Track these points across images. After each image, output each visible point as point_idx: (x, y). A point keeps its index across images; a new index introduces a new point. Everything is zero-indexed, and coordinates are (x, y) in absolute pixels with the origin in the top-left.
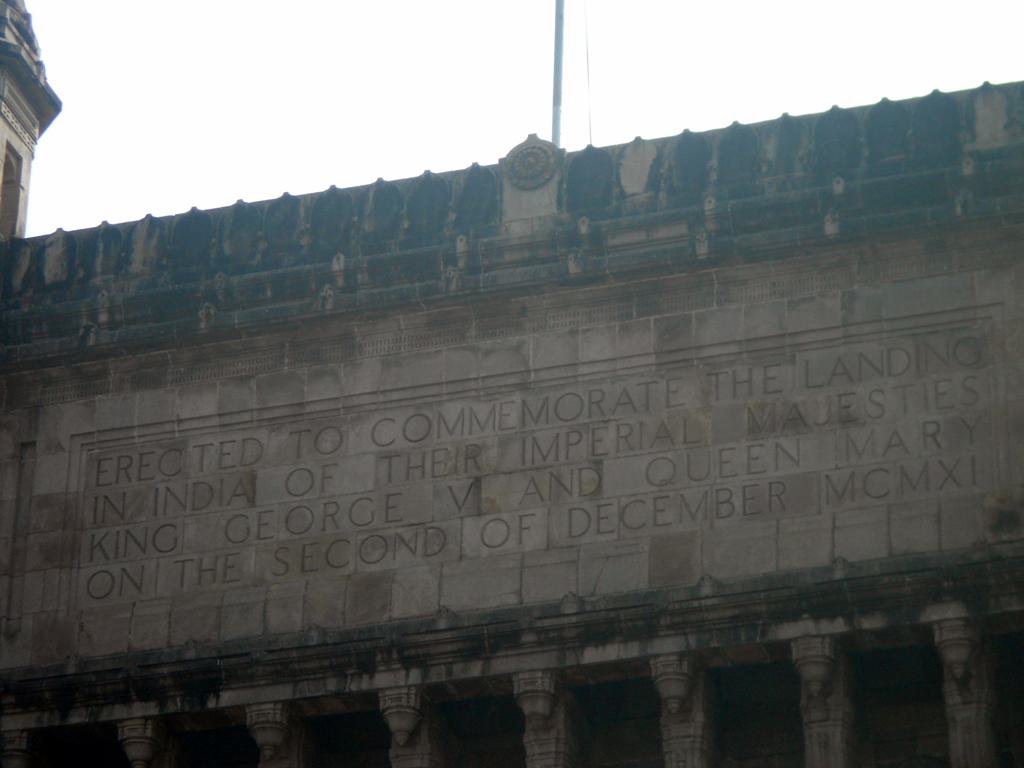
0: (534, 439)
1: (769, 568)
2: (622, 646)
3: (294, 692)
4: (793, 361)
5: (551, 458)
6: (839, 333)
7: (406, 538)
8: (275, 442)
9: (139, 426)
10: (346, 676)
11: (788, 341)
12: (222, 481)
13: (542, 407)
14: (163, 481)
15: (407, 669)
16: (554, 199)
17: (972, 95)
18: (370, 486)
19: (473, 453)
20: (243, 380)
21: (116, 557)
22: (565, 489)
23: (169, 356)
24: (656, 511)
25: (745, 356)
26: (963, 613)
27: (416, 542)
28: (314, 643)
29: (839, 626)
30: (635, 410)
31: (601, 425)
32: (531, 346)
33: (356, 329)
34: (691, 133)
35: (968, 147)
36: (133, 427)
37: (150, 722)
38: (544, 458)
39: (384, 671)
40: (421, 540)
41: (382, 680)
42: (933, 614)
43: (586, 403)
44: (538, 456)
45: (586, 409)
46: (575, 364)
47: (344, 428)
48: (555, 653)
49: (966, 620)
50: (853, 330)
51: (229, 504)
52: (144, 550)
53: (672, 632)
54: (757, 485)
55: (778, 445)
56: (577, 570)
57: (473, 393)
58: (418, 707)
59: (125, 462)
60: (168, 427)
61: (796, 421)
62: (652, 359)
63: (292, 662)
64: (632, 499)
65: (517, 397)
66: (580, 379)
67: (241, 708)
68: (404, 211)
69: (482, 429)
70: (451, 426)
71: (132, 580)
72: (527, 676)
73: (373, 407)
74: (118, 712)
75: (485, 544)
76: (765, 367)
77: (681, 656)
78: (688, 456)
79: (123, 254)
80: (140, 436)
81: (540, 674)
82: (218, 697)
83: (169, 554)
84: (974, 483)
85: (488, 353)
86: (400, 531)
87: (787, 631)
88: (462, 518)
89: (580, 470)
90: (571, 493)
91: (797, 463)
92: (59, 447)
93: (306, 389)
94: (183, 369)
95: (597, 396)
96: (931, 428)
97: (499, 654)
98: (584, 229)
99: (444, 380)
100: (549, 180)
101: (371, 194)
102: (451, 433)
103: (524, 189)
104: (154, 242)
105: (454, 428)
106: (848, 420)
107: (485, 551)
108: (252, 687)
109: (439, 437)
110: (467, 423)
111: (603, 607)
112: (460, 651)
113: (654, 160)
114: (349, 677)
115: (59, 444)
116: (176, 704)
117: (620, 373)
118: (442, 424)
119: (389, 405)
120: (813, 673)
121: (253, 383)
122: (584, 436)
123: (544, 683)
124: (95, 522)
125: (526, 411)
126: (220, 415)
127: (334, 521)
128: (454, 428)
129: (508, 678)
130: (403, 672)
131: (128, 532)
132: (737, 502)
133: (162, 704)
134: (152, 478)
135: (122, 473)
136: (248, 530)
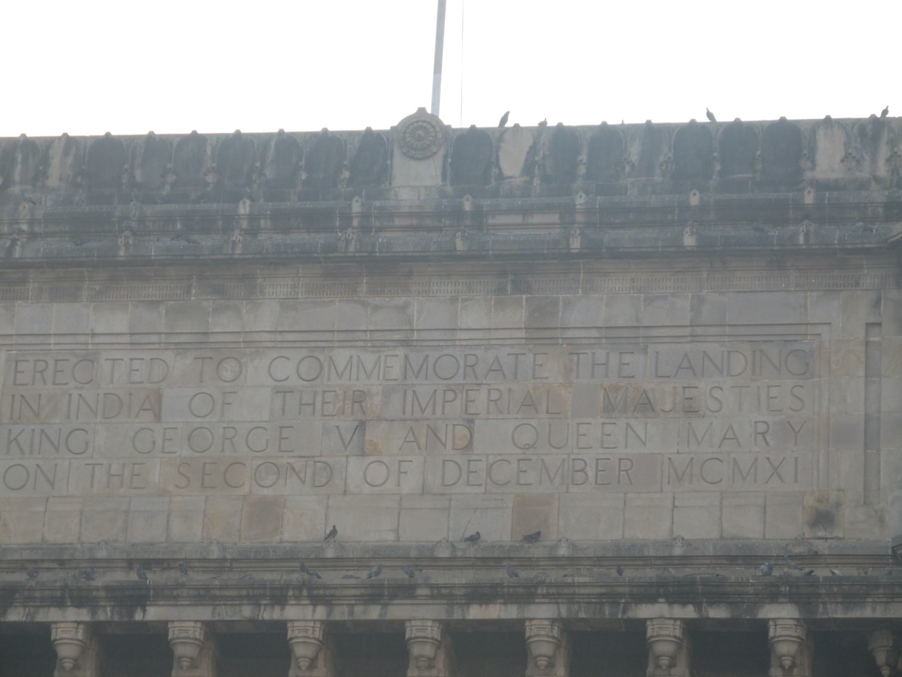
0: (414, 392)
1: (616, 535)
2: (503, 607)
3: (213, 613)
4: (645, 351)
5: (429, 410)
6: (687, 331)
9: (55, 335)
10: (259, 605)
11: (642, 332)
12: (131, 394)
14: (76, 388)
15: (315, 605)
16: (439, 172)
17: (816, 125)
19: (360, 398)
20: (153, 304)
21: (31, 452)
22: (441, 441)
25: (604, 341)
26: (796, 615)
27: (306, 473)
28: (215, 556)
29: (689, 612)
30: (505, 377)
31: (475, 387)
32: (416, 307)
33: (259, 271)
35: (808, 175)
36: (50, 335)
37: (81, 626)
38: (423, 411)
41: (291, 612)
42: (769, 612)
43: (462, 364)
44: (417, 408)
45: (461, 371)
48: (445, 606)
49: (797, 620)
50: (699, 331)
51: (136, 416)
52: (57, 450)
53: (547, 601)
54: (609, 459)
55: (628, 424)
56: (449, 516)
57: (362, 344)
58: (321, 638)
59: (41, 366)
60: (82, 339)
62: (522, 334)
63: (213, 589)
64: (499, 458)
65: (401, 352)
66: (457, 343)
67: (165, 623)
68: (303, 163)
69: (369, 377)
70: (340, 370)
71: (45, 476)
72: (419, 623)
73: (270, 344)
74: (52, 615)
75: (367, 482)
76: (620, 353)
77: (553, 621)
78: (550, 425)
79: (41, 168)
80: (55, 344)
81: (430, 623)
82: (144, 611)
83: (79, 456)
84: (796, 481)
85: (376, 308)
86: (291, 461)
87: (644, 611)
88: (347, 457)
89: (454, 425)
91: (644, 443)
93: (210, 320)
94: (98, 287)
95: (471, 360)
96: (762, 428)
97: (395, 602)
98: (467, 206)
99: (335, 329)
100: (435, 153)
101: (273, 143)
102: (340, 376)
103: (413, 158)
104: (70, 160)
105: (343, 373)
106: (690, 410)
107: (367, 489)
109: (329, 379)
110: (354, 370)
111: (472, 555)
112: (361, 595)
113: (531, 147)
114: (262, 607)
116: (107, 614)
117: (492, 342)
118: (332, 367)
119: (285, 345)
120: (664, 648)
121: (162, 309)
122: (459, 396)
123: (434, 632)
124: (11, 418)
126: (131, 334)
128: (343, 373)
129: (400, 625)
130: (311, 608)
131: (42, 431)
132: (591, 472)
133: (94, 613)
134: (66, 384)
135: (38, 376)
136: (154, 442)
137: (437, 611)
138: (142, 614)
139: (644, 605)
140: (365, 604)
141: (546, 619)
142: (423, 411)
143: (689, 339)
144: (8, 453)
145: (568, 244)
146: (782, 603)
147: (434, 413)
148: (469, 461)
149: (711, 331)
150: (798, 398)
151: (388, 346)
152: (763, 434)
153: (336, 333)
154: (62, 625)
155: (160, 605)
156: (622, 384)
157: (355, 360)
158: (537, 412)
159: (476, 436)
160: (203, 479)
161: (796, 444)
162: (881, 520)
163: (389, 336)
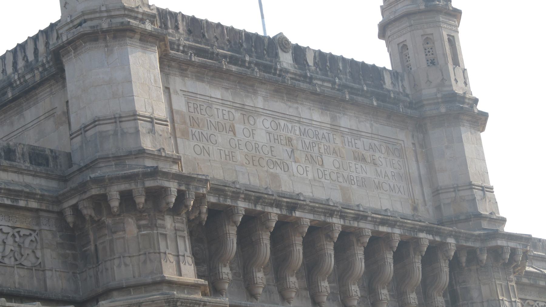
0: (304, 141)
5: (309, 150)
6: (370, 135)
8: (238, 115)
11: (359, 133)
12: (225, 124)
13: (304, 130)
14: (208, 117)
19: (290, 140)
20: (227, 89)
21: (200, 141)
23: (206, 72)
24: (338, 177)
25: (350, 134)
26: (455, 243)
33: (256, 84)
34: (365, 63)
38: (308, 149)
39: (335, 217)
40: (282, 165)
44: (306, 148)
47: (255, 118)
52: (208, 141)
53: (398, 227)
55: (361, 166)
60: (207, 98)
61: (364, 159)
64: (331, 171)
67: (299, 219)
71: (206, 151)
74: (269, 209)
80: (199, 98)
81: (370, 231)
85: (290, 107)
86: (277, 160)
87: (422, 235)
91: (366, 173)
92: (177, 92)
93: (244, 99)
95: (317, 133)
97: (361, 221)
99: (280, 112)
106: (375, 164)
107: (299, 175)
108: (303, 212)
109: (280, 131)
110: (286, 129)
112: (354, 217)
113: (314, 56)
121: (229, 91)
122: (316, 145)
125: (301, 131)
126: (222, 100)
127: (258, 149)
132: (356, 182)
136: (236, 145)
138: (294, 214)
139: (420, 233)
140: (353, 221)
141: (398, 234)
143: (370, 138)
144: (193, 139)
145: (346, 97)
146: (451, 238)
147: (311, 150)
148: (324, 170)
149: (376, 136)
150: (399, 165)
151: (294, 122)
152: (394, 176)
153: (280, 114)
155: (299, 211)
156: (357, 151)
157: (286, 125)
158: (338, 156)
159: (324, 161)
160: (253, 162)
161: (402, 182)
162: (428, 212)
163: (294, 118)
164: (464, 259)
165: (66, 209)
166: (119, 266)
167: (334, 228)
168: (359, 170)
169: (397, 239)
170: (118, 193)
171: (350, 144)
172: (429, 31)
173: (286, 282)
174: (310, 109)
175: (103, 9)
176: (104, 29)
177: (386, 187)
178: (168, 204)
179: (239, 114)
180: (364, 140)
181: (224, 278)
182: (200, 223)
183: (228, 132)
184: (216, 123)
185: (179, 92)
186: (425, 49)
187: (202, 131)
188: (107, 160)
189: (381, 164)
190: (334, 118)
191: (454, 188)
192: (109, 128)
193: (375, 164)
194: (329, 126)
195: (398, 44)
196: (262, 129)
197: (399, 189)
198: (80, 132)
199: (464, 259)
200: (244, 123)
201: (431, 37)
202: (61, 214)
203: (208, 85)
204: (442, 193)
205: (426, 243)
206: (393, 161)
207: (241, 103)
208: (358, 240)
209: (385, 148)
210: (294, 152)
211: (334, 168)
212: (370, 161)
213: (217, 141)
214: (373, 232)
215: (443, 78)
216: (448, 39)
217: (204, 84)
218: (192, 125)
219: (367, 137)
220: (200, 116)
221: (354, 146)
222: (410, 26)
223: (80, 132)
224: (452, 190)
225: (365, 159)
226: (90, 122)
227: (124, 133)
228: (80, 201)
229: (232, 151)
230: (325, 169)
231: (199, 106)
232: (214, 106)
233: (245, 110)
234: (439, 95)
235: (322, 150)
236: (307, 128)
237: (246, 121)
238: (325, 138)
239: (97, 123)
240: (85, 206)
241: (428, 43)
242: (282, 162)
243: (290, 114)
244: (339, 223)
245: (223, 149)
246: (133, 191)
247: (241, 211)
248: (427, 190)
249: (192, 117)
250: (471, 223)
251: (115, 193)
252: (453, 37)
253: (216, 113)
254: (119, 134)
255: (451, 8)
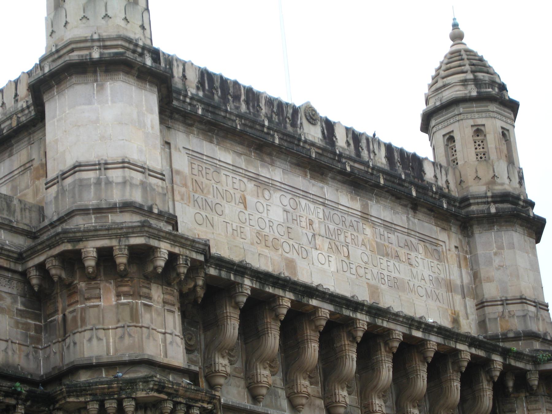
5: (334, 237)
6: (406, 230)
7: (296, 248)
8: (250, 186)
11: (393, 226)
12: (234, 193)
18: (282, 221)
19: (311, 223)
25: (382, 225)
40: (300, 249)
41: (359, 316)
44: (330, 235)
46: (338, 204)
50: (409, 232)
52: (212, 210)
64: (359, 265)
65: (321, 207)
66: (339, 210)
67: (316, 309)
81: (401, 334)
85: (313, 185)
86: (294, 244)
90: (341, 253)
91: (399, 273)
95: (344, 219)
102: (303, 211)
106: (411, 264)
109: (300, 211)
115: (179, 149)
117: (350, 214)
121: (242, 157)
126: (233, 166)
127: (272, 228)
132: (386, 280)
136: (246, 219)
137: (405, 330)
142: (332, 236)
143: (406, 234)
144: (194, 206)
147: (336, 238)
154: (285, 299)
157: (307, 206)
164: (511, 384)
165: (32, 269)
166: (90, 340)
167: (358, 325)
168: (391, 268)
169: (432, 348)
170: (95, 250)
171: (382, 237)
172: (480, 122)
173: (297, 385)
174: (337, 190)
175: (96, 37)
176: (95, 60)
177: (422, 292)
178: (155, 268)
179: (253, 185)
180: (399, 235)
181: (220, 370)
182: (196, 301)
183: (237, 203)
184: (224, 191)
185: (181, 149)
186: (475, 142)
187: (206, 198)
188: (86, 212)
189: (417, 265)
190: (365, 206)
191: (501, 300)
192: (91, 175)
193: (411, 264)
194: (359, 214)
195: (444, 136)
196: (279, 206)
197: (437, 297)
198: (56, 181)
199: (511, 384)
200: (258, 197)
201: (482, 128)
202: (24, 274)
203: (218, 146)
204: (488, 306)
205: (467, 357)
206: (432, 263)
207: (255, 172)
208: (386, 344)
209: (423, 247)
210: (315, 238)
211: (361, 262)
212: (404, 260)
213: (224, 212)
214: (404, 335)
215: (495, 175)
216: (503, 132)
217: (212, 145)
218: (195, 190)
219: (403, 233)
220: (204, 180)
221: (387, 241)
222: (458, 115)
223: (56, 181)
224: (499, 303)
225: (398, 256)
226: (69, 168)
227: (109, 183)
228: (49, 258)
229: (241, 226)
230: (351, 262)
231: (204, 168)
232: (223, 172)
233: (260, 181)
234: (489, 194)
235: (349, 240)
236: (333, 212)
237: (260, 195)
238: (353, 226)
239: (77, 169)
240: (54, 264)
241: (478, 136)
242: (300, 247)
243: (313, 193)
244: (365, 320)
245: (230, 222)
246: (114, 248)
247: (246, 290)
248: (471, 303)
249: (195, 180)
250: (520, 343)
251: (92, 249)
252: (508, 130)
253: (225, 180)
254: (103, 183)
255: (507, 98)
